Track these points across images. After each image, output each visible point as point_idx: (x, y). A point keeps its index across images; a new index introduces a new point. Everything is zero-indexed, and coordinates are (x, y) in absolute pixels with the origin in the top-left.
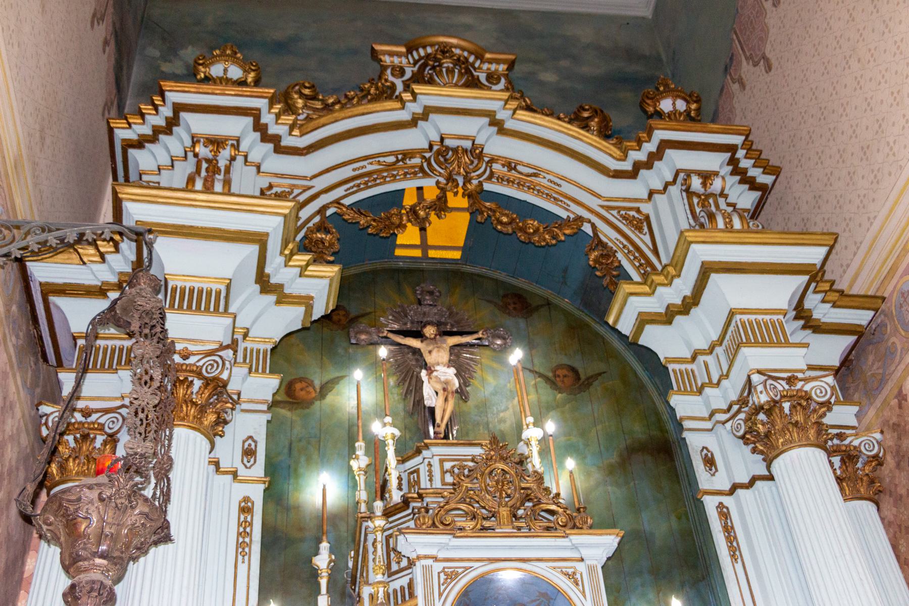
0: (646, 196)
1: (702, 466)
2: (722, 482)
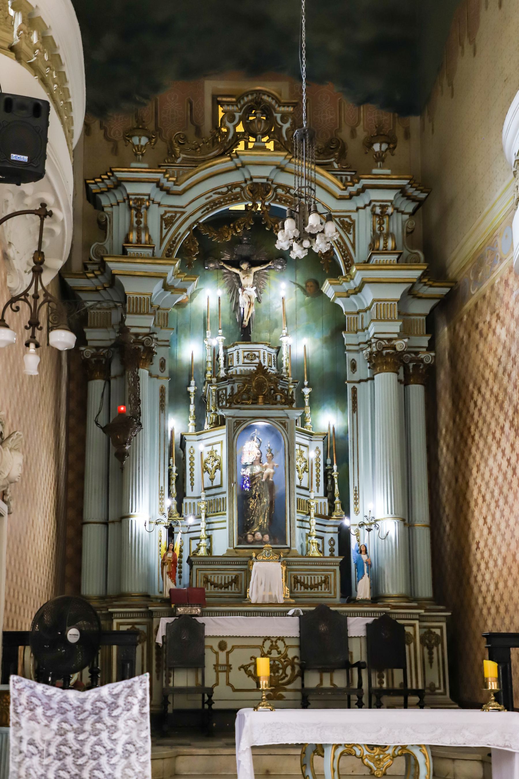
0: (355, 209)
1: (350, 369)
2: (357, 376)
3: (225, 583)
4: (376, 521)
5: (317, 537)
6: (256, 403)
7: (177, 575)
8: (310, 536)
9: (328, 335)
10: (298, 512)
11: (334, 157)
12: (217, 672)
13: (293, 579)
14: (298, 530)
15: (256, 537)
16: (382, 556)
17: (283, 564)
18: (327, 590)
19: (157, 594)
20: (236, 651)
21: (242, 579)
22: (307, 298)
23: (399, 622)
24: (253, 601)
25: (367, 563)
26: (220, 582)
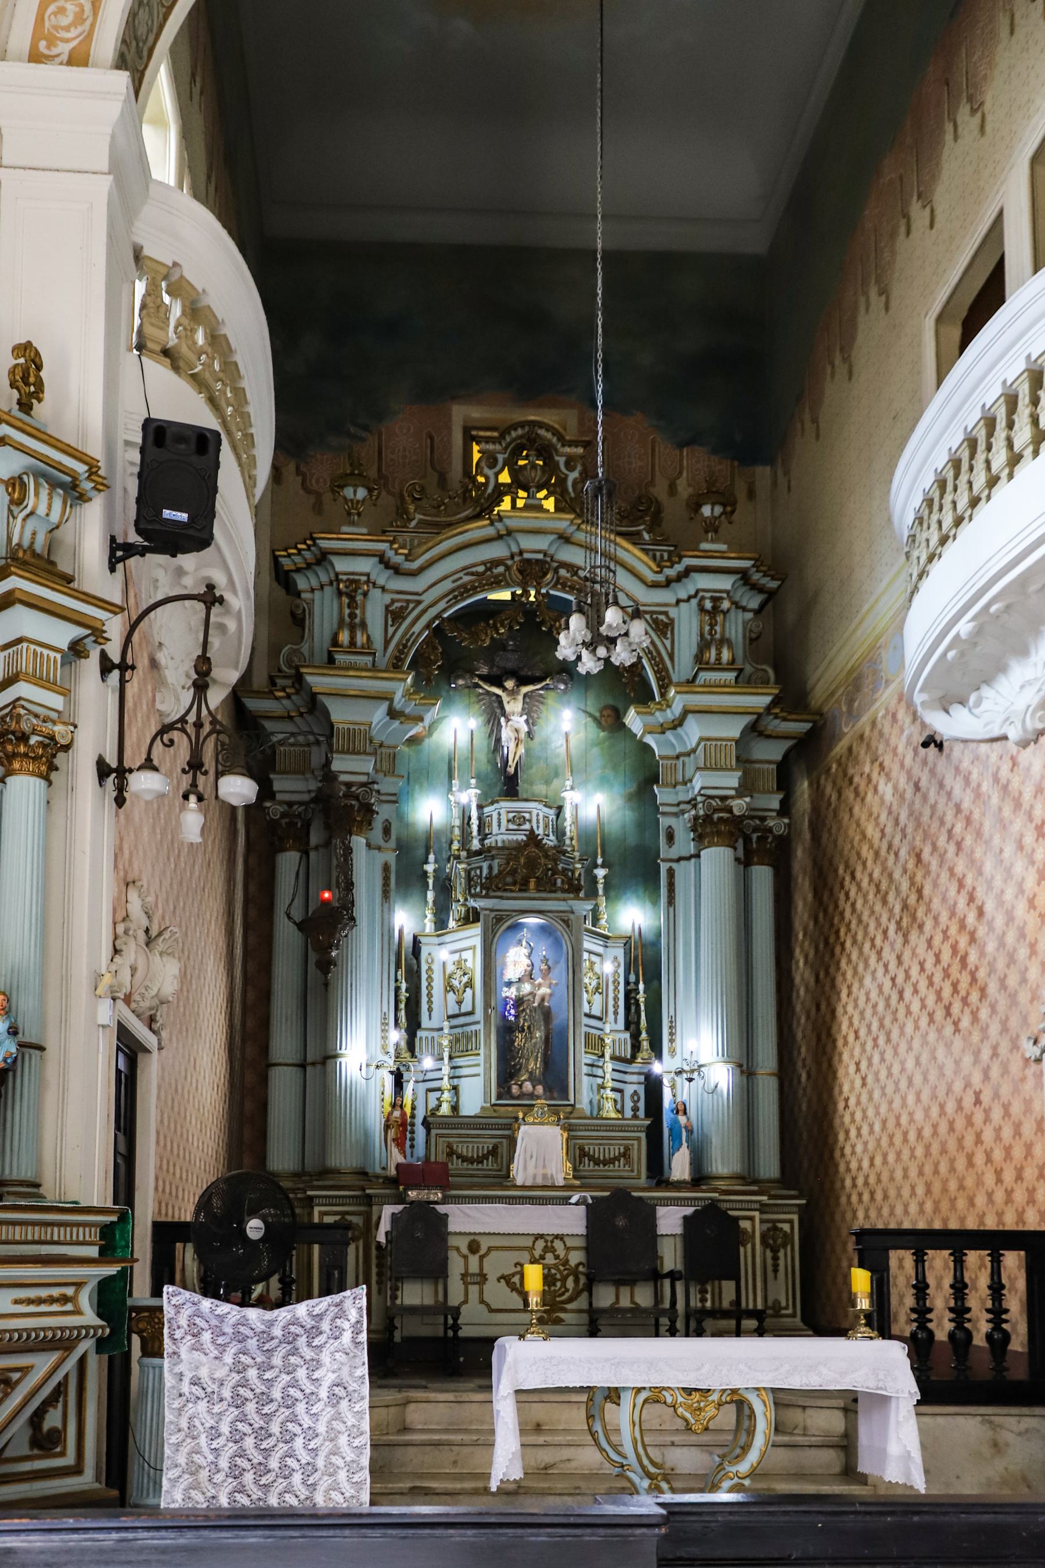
2: (674, 852)
3: (478, 1156)
4: (700, 1066)
5: (613, 1090)
6: (525, 891)
7: (408, 1143)
8: (604, 1088)
9: (632, 790)
10: (586, 1052)
11: (644, 523)
12: (466, 1284)
14: (585, 1080)
15: (524, 1089)
16: (708, 1118)
17: (564, 1128)
18: (627, 1168)
19: (378, 1170)
20: (493, 1253)
21: (504, 1150)
22: (602, 734)
23: (731, 1213)
24: (519, 1182)
25: (686, 1127)
26: (470, 1155)
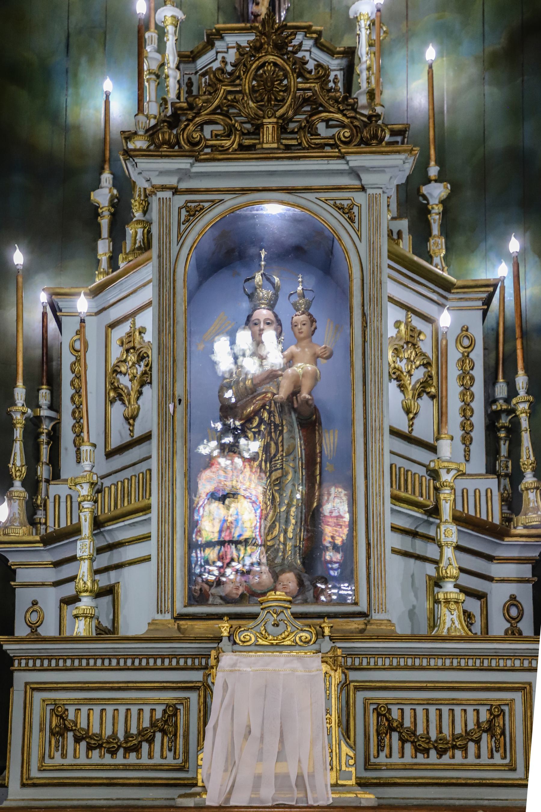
3: (128, 735)
9: (498, 47)
13: (373, 719)
18: (497, 759)
26: (108, 732)
